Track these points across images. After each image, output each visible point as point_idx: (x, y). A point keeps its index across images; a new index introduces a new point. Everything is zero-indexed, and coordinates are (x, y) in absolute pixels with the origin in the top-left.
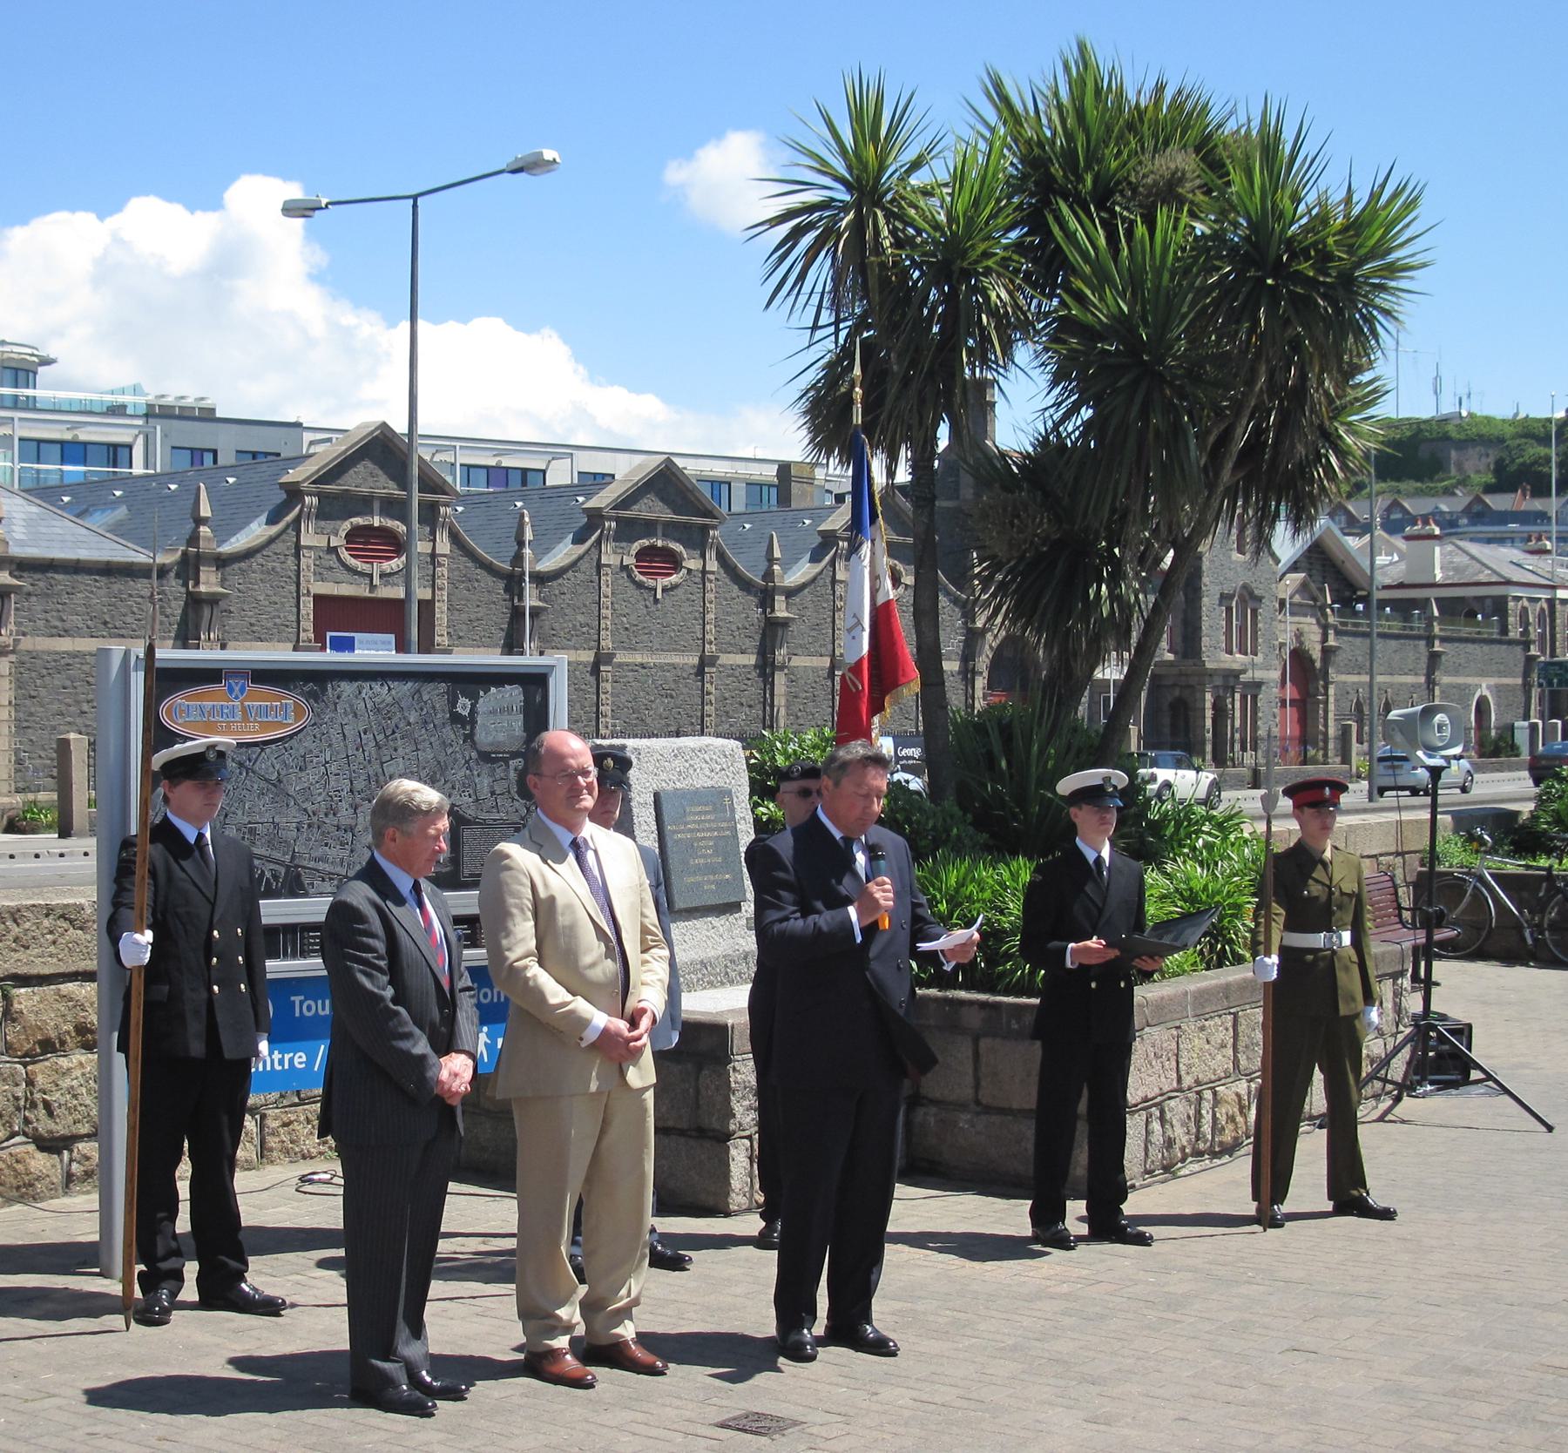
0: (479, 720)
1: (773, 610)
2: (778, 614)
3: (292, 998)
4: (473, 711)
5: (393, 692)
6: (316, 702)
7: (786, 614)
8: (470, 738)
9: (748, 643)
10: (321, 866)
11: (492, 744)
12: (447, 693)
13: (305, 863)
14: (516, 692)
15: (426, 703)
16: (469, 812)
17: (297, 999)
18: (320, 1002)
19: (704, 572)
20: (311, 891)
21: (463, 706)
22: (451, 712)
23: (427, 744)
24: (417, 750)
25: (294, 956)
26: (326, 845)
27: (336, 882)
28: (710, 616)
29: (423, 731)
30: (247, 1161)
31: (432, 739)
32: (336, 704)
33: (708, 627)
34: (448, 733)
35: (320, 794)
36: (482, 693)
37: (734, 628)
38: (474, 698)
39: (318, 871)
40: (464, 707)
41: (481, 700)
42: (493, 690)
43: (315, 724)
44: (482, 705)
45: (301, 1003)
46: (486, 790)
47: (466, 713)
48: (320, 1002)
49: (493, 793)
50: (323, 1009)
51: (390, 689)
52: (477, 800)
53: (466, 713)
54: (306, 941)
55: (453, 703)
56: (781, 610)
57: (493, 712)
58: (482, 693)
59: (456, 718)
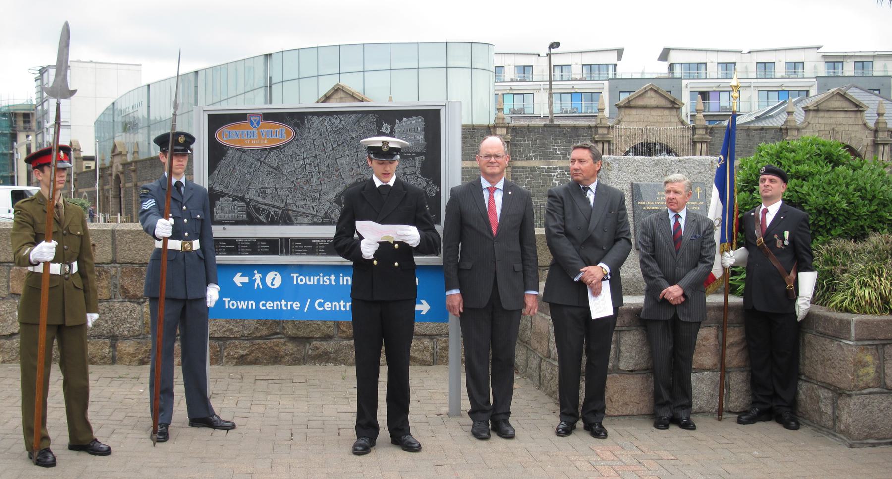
3: (292, 275)
5: (343, 122)
6: (299, 128)
10: (302, 210)
13: (293, 208)
17: (295, 275)
18: (307, 278)
20: (295, 222)
25: (287, 254)
26: (304, 199)
27: (310, 218)
32: (309, 129)
35: (301, 174)
39: (300, 212)
43: (297, 139)
45: (297, 277)
48: (307, 278)
50: (310, 281)
51: (341, 121)
54: (293, 247)
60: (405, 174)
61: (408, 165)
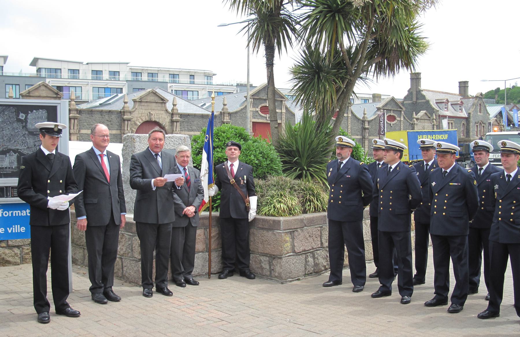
0: (29, 121)
1: (365, 126)
2: (366, 127)
4: (26, 118)
7: (368, 127)
8: (25, 127)
9: (359, 133)
11: (33, 129)
12: (15, 112)
14: (44, 112)
15: (6, 115)
16: (25, 152)
19: (348, 117)
21: (22, 116)
22: (17, 118)
23: (7, 129)
24: (3, 131)
28: (349, 127)
29: (5, 124)
30: (15, 262)
31: (9, 127)
33: (349, 130)
34: (15, 125)
36: (30, 112)
37: (355, 130)
38: (27, 114)
40: (22, 117)
41: (29, 115)
42: (34, 111)
44: (30, 116)
46: (32, 144)
47: (23, 119)
49: (35, 145)
52: (28, 148)
53: (23, 119)
55: (18, 115)
56: (367, 126)
57: (35, 119)
58: (30, 112)
59: (19, 120)
60: (35, 145)
61: (37, 140)
